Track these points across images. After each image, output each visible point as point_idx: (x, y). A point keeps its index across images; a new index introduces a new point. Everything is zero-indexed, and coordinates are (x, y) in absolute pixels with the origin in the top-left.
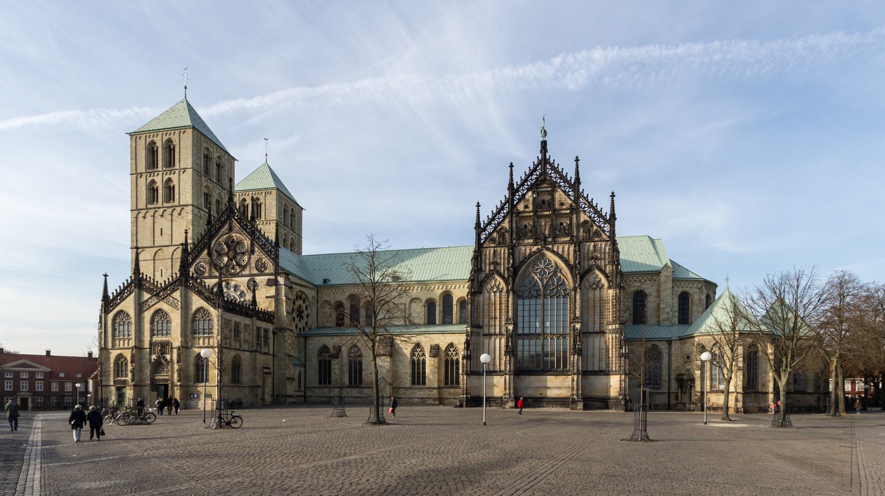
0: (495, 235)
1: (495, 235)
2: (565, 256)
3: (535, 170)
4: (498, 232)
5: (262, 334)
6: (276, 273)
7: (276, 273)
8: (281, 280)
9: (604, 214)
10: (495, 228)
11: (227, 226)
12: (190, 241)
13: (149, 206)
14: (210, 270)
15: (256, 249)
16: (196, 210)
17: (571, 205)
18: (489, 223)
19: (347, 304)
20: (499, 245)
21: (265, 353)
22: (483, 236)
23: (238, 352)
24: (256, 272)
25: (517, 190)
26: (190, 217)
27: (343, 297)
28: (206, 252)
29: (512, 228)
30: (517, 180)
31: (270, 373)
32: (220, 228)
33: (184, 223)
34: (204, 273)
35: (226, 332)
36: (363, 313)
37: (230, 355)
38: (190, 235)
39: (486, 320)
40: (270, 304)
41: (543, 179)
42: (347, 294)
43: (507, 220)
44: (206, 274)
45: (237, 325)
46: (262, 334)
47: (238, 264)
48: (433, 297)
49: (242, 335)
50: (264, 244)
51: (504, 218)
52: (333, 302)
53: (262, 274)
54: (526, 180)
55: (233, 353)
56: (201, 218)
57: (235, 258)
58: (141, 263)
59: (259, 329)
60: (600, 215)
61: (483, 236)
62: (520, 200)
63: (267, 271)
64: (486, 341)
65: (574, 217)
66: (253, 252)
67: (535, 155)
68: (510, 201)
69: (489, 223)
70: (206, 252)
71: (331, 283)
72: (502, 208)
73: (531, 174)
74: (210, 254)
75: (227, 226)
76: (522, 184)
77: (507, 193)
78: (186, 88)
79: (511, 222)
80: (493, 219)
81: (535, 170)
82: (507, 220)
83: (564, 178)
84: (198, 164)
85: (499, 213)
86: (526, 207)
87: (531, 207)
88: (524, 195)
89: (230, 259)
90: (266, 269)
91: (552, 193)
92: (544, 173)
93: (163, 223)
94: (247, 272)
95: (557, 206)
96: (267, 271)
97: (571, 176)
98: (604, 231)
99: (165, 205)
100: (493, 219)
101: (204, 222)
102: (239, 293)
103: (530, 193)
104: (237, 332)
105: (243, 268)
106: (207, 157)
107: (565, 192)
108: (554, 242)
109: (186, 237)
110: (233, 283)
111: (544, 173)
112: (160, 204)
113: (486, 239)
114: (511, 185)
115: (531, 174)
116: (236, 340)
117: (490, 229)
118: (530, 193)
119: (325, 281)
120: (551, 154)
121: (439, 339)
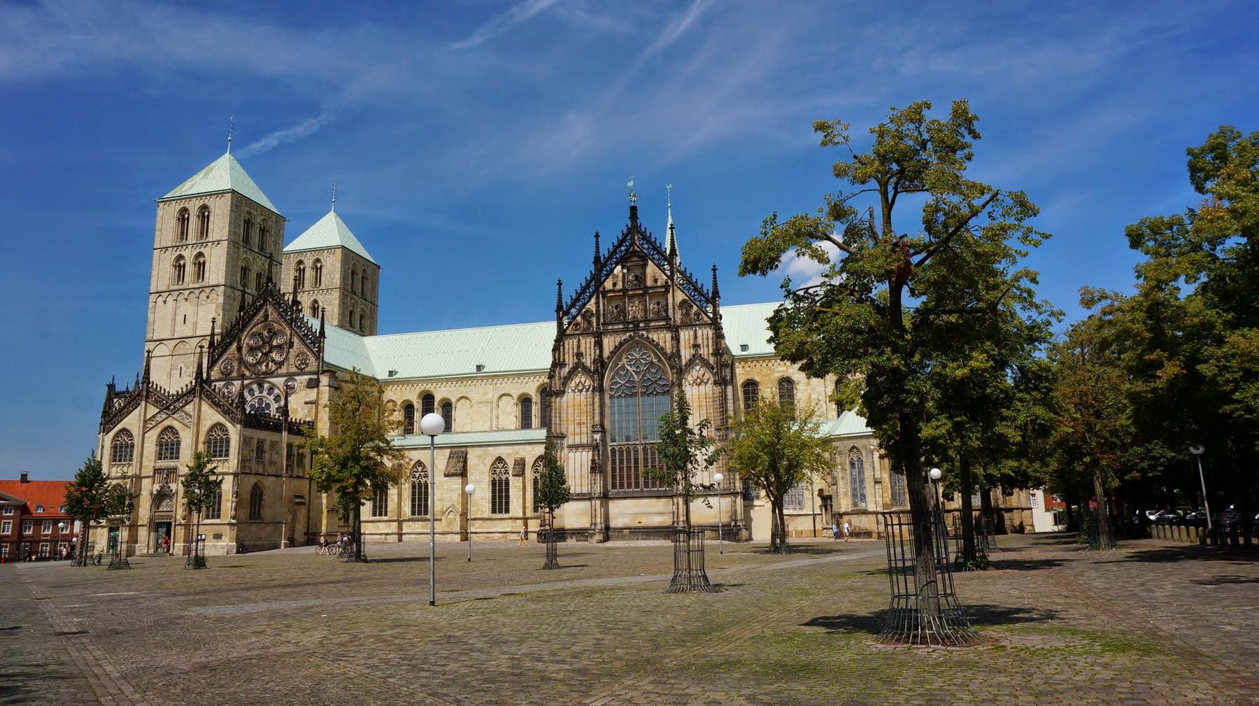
0: (579, 318)
1: (579, 318)
2: (662, 344)
3: (624, 240)
4: (584, 317)
8: (324, 380)
10: (580, 311)
11: (262, 313)
12: (217, 331)
13: (172, 288)
14: (239, 369)
16: (229, 290)
18: (573, 305)
20: (586, 333)
21: (298, 477)
23: (260, 478)
25: (605, 265)
26: (221, 300)
27: (412, 395)
28: (235, 345)
29: (598, 310)
30: (604, 252)
32: (255, 315)
33: (214, 306)
35: (246, 453)
38: (219, 321)
39: (571, 427)
40: (310, 411)
43: (593, 300)
44: (234, 374)
45: (261, 443)
47: (273, 361)
49: (267, 456)
50: (306, 335)
51: (590, 298)
52: (399, 403)
53: (301, 372)
54: (614, 252)
55: (253, 480)
56: (235, 299)
58: (153, 361)
60: (701, 294)
61: (565, 321)
62: (607, 276)
65: (670, 294)
69: (573, 305)
70: (235, 345)
72: (588, 286)
73: (620, 245)
74: (239, 349)
75: (262, 313)
76: (610, 257)
77: (592, 268)
79: (597, 303)
80: (578, 299)
81: (624, 240)
82: (593, 300)
84: (235, 233)
85: (583, 292)
86: (615, 285)
87: (620, 286)
88: (612, 270)
90: (307, 365)
93: (186, 308)
94: (283, 370)
95: (649, 283)
99: (191, 286)
100: (578, 299)
101: (237, 305)
103: (619, 267)
105: (280, 364)
106: (248, 223)
107: (659, 266)
108: (647, 329)
109: (213, 328)
112: (185, 286)
113: (569, 324)
114: (597, 259)
115: (620, 245)
116: (258, 463)
117: (573, 311)
118: (619, 267)
119: (391, 373)
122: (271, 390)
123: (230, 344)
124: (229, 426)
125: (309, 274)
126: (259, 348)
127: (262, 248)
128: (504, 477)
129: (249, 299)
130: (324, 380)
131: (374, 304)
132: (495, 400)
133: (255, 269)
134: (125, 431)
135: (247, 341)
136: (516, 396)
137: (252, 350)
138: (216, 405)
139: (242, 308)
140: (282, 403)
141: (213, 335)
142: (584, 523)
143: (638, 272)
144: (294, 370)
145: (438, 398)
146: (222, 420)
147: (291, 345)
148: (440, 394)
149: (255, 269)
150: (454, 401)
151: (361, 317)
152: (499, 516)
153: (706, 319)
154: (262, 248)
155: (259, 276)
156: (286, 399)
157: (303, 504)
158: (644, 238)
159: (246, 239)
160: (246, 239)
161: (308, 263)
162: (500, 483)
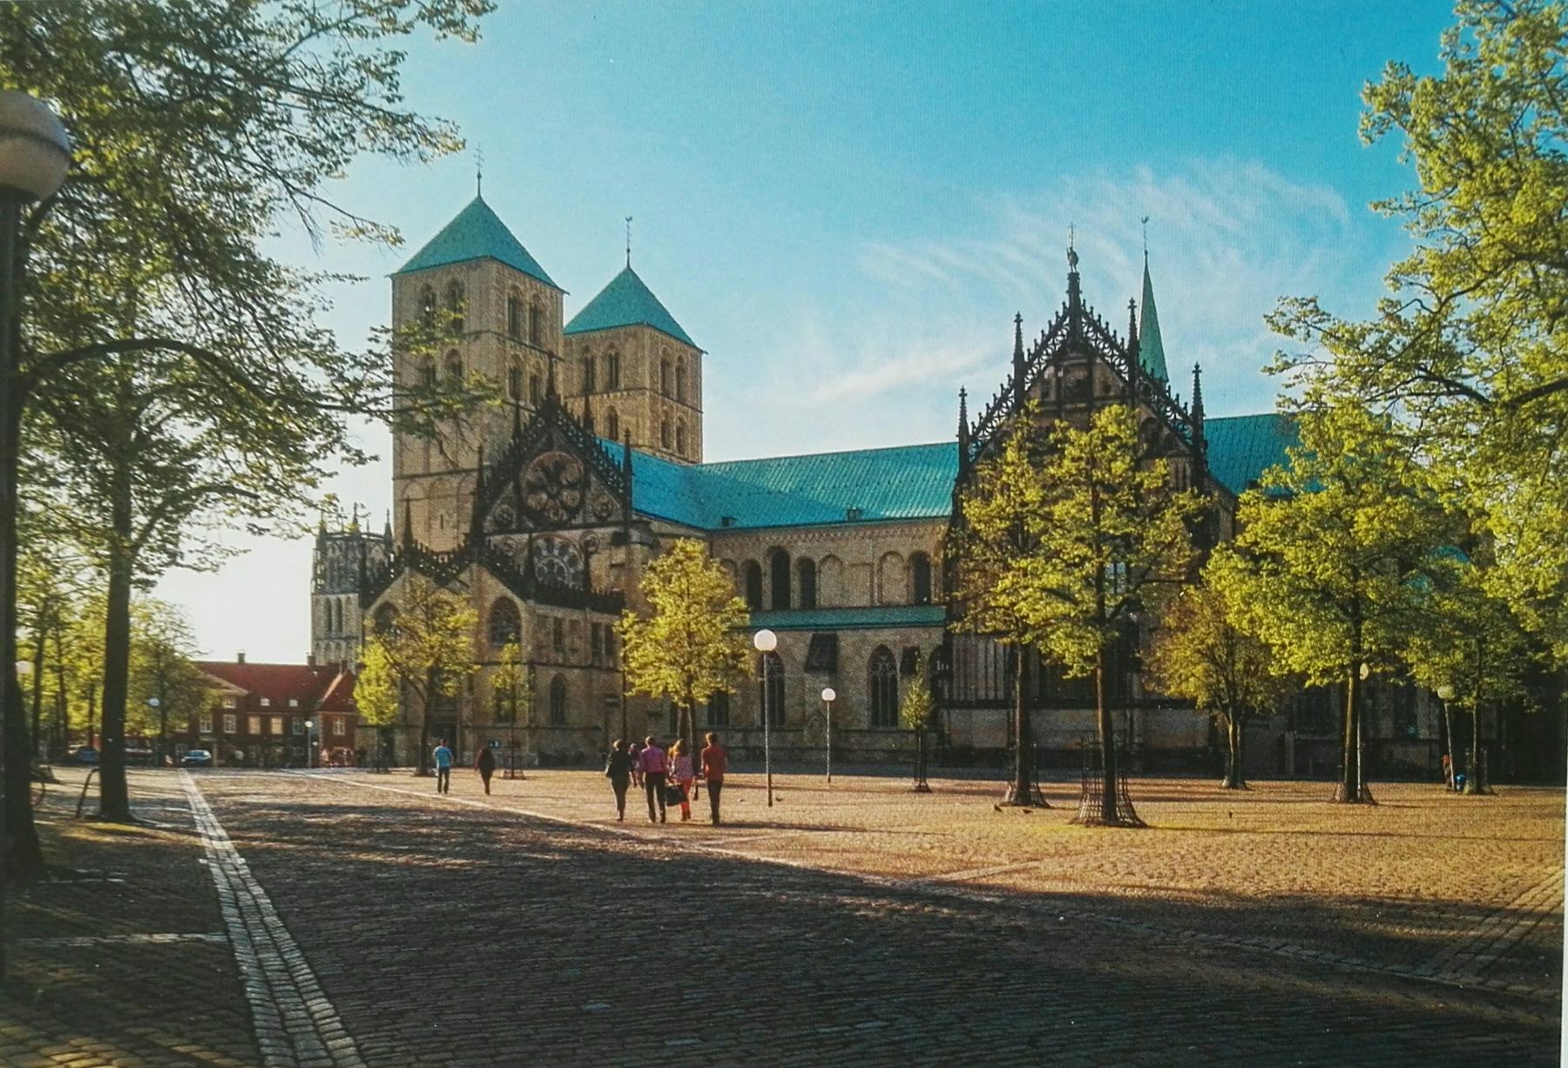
3: (1059, 326)
5: (602, 634)
6: (627, 523)
7: (627, 523)
9: (1182, 405)
14: (519, 516)
15: (593, 479)
17: (1123, 390)
19: (766, 567)
22: (973, 450)
24: (593, 520)
25: (1030, 365)
28: (511, 485)
30: (1028, 345)
31: (616, 705)
32: (534, 441)
34: (510, 523)
36: (795, 584)
37: (546, 676)
40: (617, 578)
41: (1075, 342)
42: (765, 547)
46: (602, 634)
48: (923, 548)
49: (567, 641)
53: (603, 522)
54: (1044, 345)
55: (553, 672)
57: (559, 493)
59: (596, 626)
63: (612, 519)
64: (981, 646)
66: (582, 484)
67: (1060, 298)
68: (1017, 383)
70: (511, 485)
71: (738, 524)
72: (1004, 398)
74: (517, 489)
76: (1038, 354)
78: (479, 176)
83: (1110, 340)
85: (998, 406)
87: (1052, 397)
89: (551, 497)
91: (1089, 366)
92: (1075, 329)
94: (579, 520)
95: (1098, 392)
96: (612, 519)
97: (1123, 336)
98: (1183, 438)
102: (566, 558)
103: (1051, 369)
104: (558, 635)
105: (573, 512)
109: (481, 460)
110: (557, 541)
111: (1075, 329)
113: (977, 454)
119: (725, 520)
120: (1091, 297)
121: (918, 636)
122: (564, 549)
123: (505, 483)
124: (517, 600)
125: (600, 368)
126: (543, 488)
127: (535, 338)
128: (889, 675)
129: (525, 416)
130: (635, 535)
131: (697, 410)
132: (876, 562)
133: (529, 370)
134: (388, 606)
135: (529, 476)
136: (906, 556)
137: (534, 488)
138: (497, 573)
139: (517, 433)
140: (581, 567)
141: (481, 469)
142: (998, 740)
143: (1080, 374)
144: (593, 520)
145: (795, 556)
146: (510, 594)
147: (587, 485)
148: (799, 549)
149: (529, 370)
150: (817, 561)
151: (679, 430)
152: (881, 728)
153: (1183, 448)
154: (535, 338)
155: (535, 380)
156: (587, 564)
157: (616, 705)
158: (1091, 323)
159: (514, 329)
160: (514, 329)
161: (598, 352)
162: (884, 684)
